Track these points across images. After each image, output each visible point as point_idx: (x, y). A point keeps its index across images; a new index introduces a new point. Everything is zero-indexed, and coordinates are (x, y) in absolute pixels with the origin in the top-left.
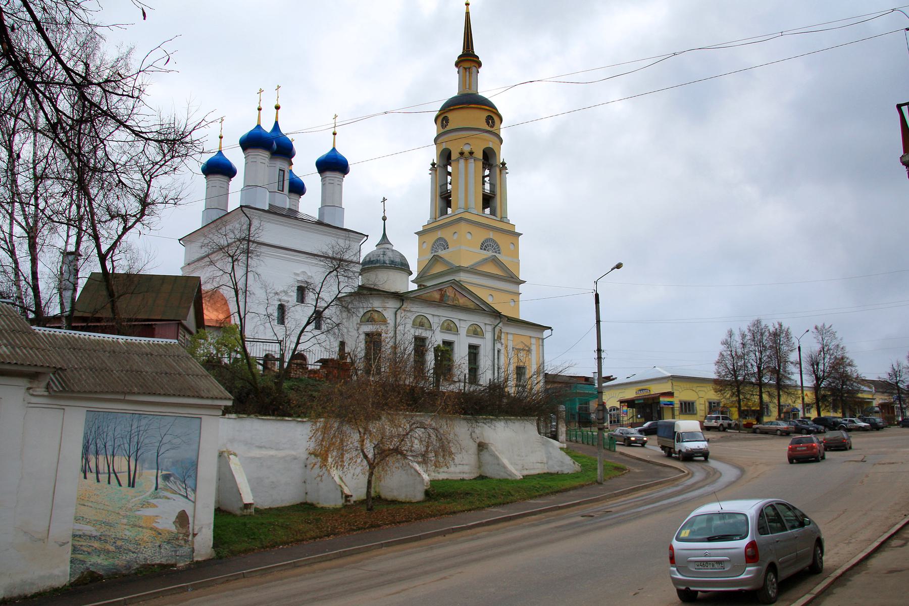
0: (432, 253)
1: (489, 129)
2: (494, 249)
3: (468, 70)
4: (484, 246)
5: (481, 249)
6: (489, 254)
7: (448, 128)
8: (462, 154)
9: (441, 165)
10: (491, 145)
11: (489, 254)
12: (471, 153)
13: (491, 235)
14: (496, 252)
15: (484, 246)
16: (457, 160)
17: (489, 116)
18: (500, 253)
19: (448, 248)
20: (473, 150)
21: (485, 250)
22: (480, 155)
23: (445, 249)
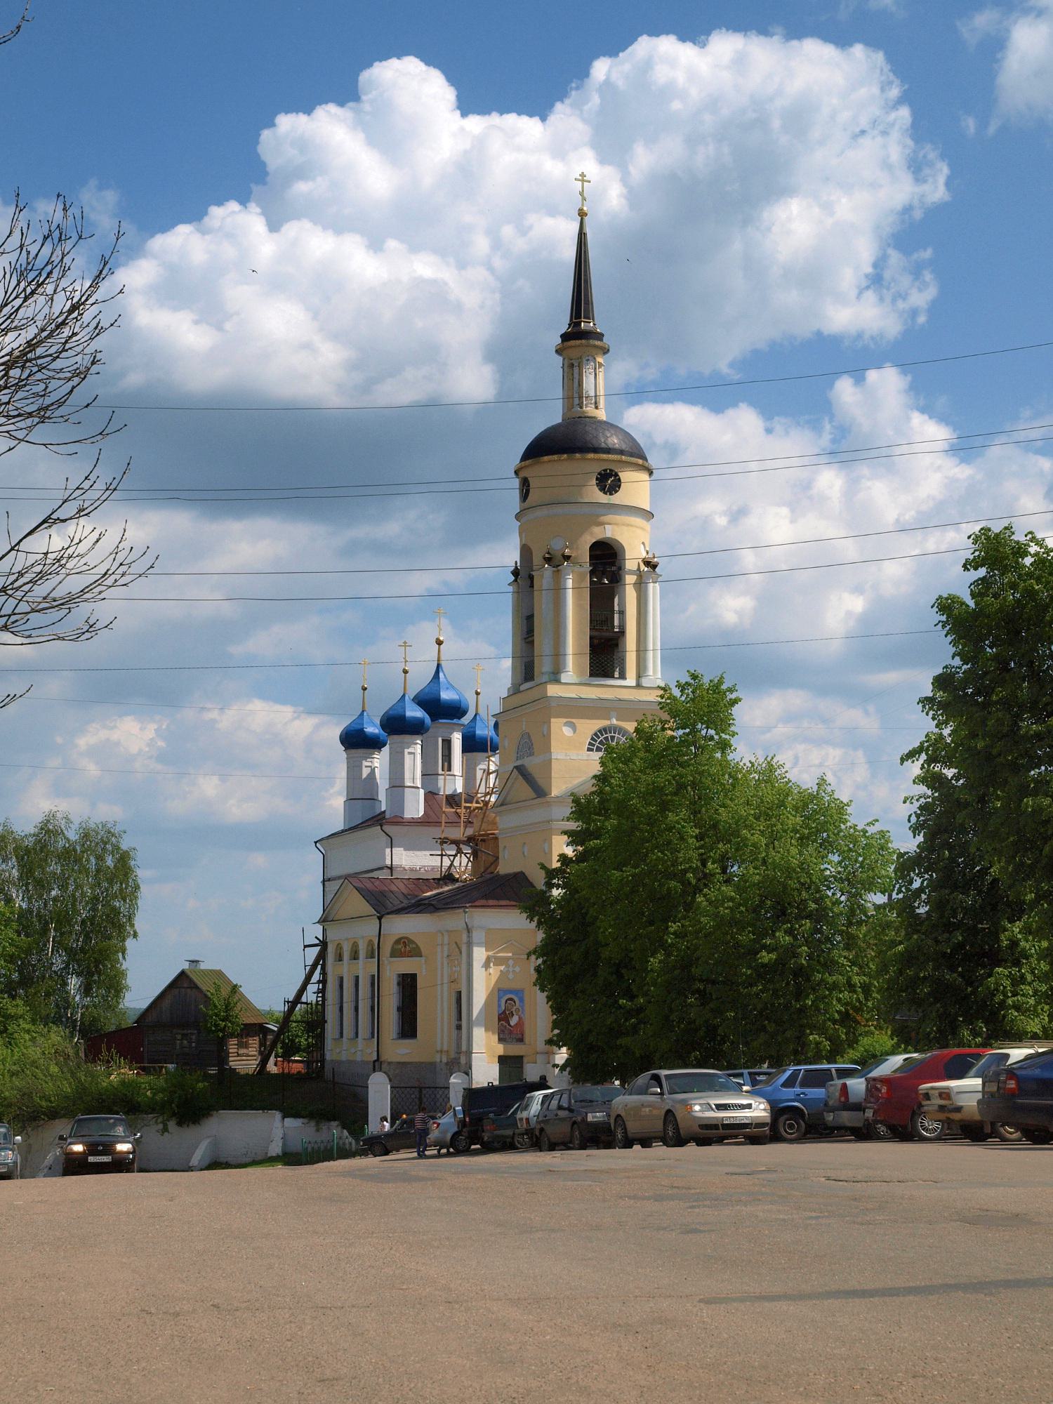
5: (589, 750)
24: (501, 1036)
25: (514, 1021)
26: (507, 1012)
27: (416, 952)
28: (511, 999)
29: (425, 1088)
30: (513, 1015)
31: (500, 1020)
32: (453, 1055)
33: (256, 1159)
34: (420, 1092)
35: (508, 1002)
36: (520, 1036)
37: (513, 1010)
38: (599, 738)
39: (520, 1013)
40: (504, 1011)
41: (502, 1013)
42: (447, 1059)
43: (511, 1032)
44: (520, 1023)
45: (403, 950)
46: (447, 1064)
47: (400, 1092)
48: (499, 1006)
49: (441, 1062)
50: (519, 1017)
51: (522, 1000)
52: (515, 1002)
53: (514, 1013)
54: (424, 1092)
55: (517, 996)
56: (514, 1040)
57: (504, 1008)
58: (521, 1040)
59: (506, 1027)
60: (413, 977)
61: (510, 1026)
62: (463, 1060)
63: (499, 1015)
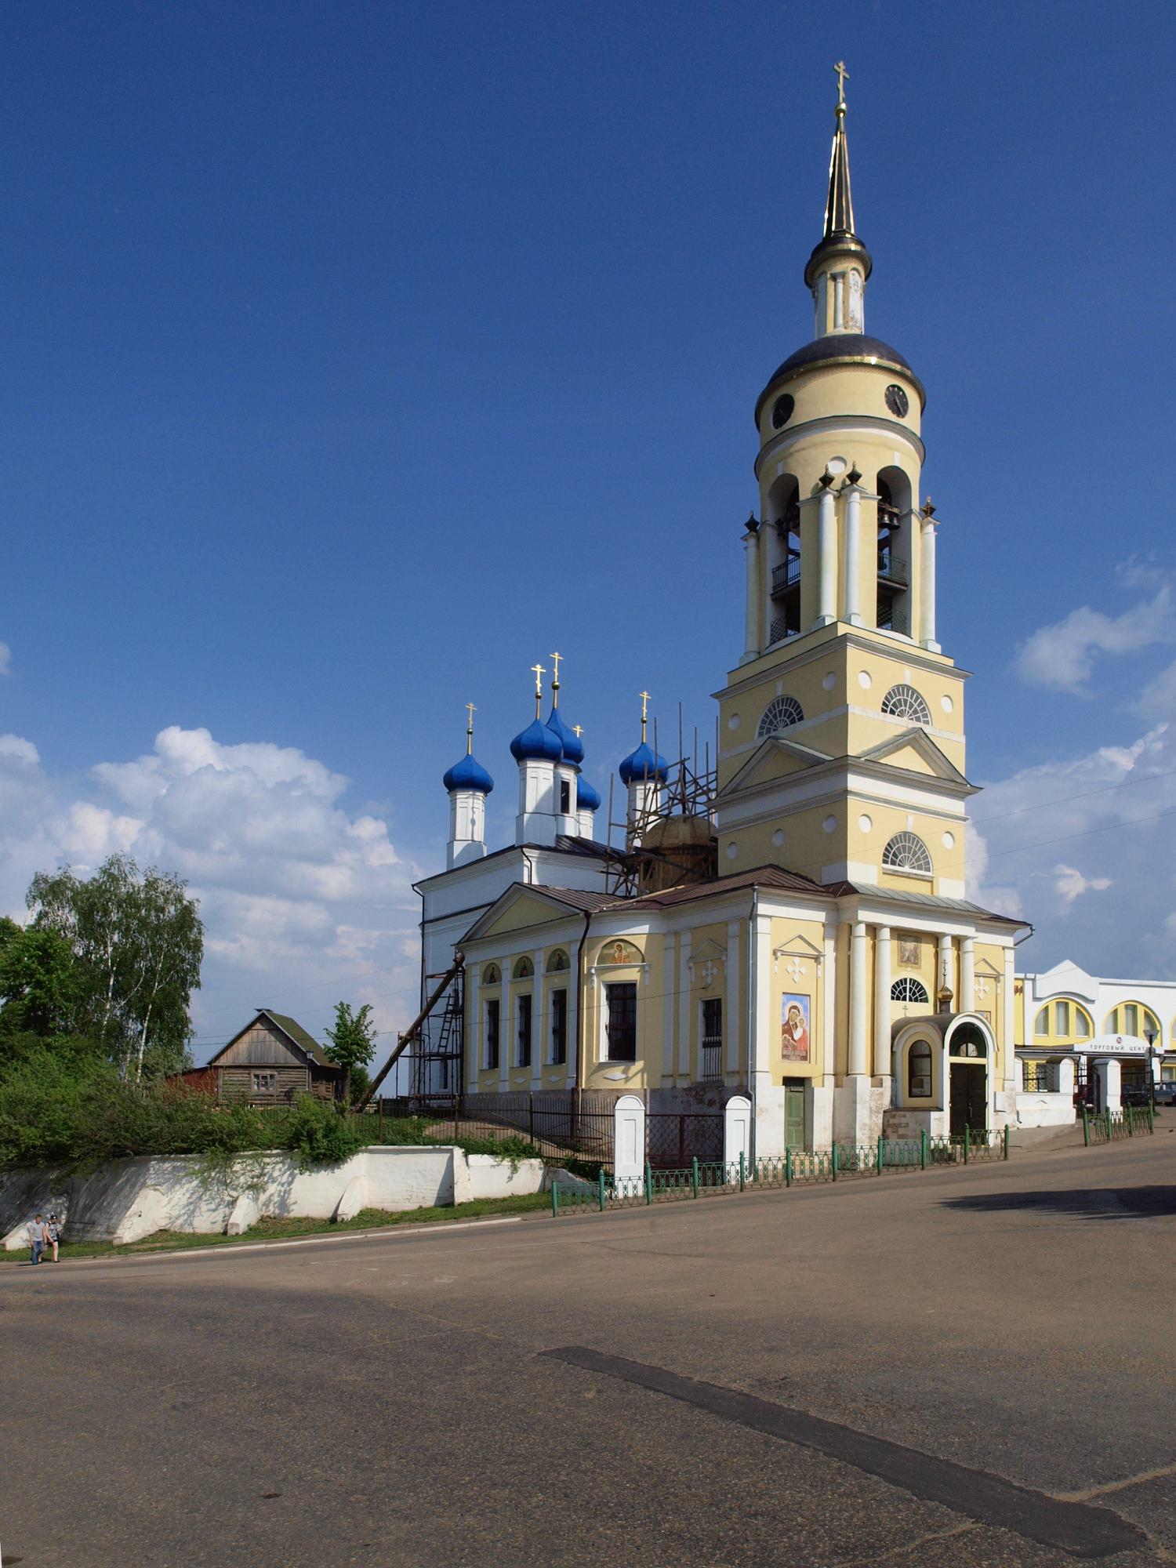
1: (893, 418)
4: (890, 706)
5: (884, 711)
6: (900, 725)
10: (897, 461)
11: (900, 725)
13: (909, 675)
14: (918, 719)
15: (890, 706)
17: (893, 386)
18: (927, 722)
19: (801, 719)
20: (859, 470)
21: (892, 712)
22: (869, 483)
23: (793, 722)
24: (785, 1053)
25: (797, 1034)
26: (791, 1024)
28: (795, 1007)
30: (797, 1027)
31: (784, 1032)
32: (700, 1079)
33: (424, 1206)
35: (792, 1010)
37: (797, 1021)
38: (892, 699)
39: (804, 1025)
40: (787, 1023)
41: (785, 1024)
43: (794, 1048)
44: (803, 1039)
45: (616, 956)
48: (783, 1014)
50: (804, 1031)
52: (799, 1011)
53: (798, 1024)
54: (687, 1121)
58: (804, 1058)
59: (789, 1040)
61: (793, 1039)
62: (730, 1082)
63: (784, 1025)
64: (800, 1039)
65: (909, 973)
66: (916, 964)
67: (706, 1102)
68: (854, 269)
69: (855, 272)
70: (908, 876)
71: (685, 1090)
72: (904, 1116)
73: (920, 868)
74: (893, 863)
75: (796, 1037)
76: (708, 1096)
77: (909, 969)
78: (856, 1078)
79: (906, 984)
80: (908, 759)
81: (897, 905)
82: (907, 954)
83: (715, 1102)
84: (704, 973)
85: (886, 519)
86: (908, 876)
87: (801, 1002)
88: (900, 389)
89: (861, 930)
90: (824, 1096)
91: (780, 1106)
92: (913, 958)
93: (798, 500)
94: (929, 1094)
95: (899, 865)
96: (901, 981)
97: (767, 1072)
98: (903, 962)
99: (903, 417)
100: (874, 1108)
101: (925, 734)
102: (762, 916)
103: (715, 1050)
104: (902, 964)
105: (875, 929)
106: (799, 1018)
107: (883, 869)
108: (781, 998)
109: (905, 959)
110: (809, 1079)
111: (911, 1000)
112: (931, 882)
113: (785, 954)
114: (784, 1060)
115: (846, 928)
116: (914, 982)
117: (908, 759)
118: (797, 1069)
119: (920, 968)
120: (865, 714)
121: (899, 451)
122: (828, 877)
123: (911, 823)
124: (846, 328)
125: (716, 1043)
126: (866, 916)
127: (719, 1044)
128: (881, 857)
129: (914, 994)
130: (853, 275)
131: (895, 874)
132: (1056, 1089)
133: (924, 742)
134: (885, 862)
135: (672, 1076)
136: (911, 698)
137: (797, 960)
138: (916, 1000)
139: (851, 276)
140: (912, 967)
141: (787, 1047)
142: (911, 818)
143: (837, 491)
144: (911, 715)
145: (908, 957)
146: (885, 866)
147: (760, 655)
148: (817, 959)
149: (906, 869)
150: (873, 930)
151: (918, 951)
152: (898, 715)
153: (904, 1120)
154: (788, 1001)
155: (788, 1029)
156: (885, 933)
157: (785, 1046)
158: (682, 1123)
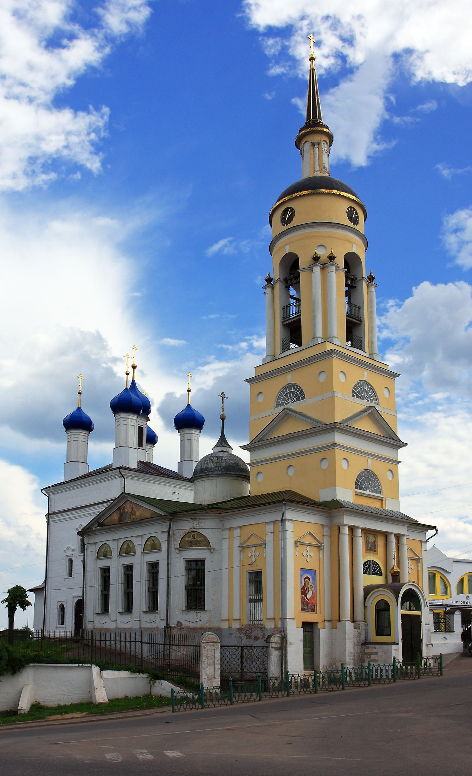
0: (277, 406)
1: (351, 225)
2: (368, 399)
3: (316, 145)
4: (357, 393)
5: (353, 396)
6: (361, 404)
7: (292, 224)
8: (316, 259)
9: (282, 280)
12: (332, 258)
15: (357, 393)
16: (310, 269)
17: (351, 207)
19: (304, 398)
22: (340, 261)
23: (298, 399)
25: (309, 595)
26: (306, 588)
27: (205, 544)
28: (307, 578)
29: (247, 647)
34: (242, 650)
35: (306, 579)
36: (313, 607)
37: (309, 586)
39: (313, 589)
40: (304, 587)
42: (240, 625)
43: (308, 604)
44: (314, 597)
46: (240, 629)
47: (230, 650)
49: (230, 628)
51: (314, 579)
55: (311, 576)
56: (310, 610)
57: (303, 585)
58: (314, 610)
60: (203, 562)
61: (307, 598)
63: (301, 589)
64: (311, 598)
65: (371, 557)
66: (375, 551)
67: (253, 637)
68: (324, 141)
69: (325, 143)
70: (369, 497)
71: (238, 629)
72: (375, 648)
73: (375, 492)
74: (361, 489)
75: (309, 597)
76: (253, 635)
77: (371, 554)
78: (345, 623)
79: (370, 564)
80: (366, 425)
81: (365, 514)
82: (370, 545)
83: (259, 637)
84: (250, 555)
85: (349, 282)
86: (369, 497)
87: (311, 574)
88: (354, 209)
89: (346, 530)
90: (323, 633)
91: (301, 641)
92: (373, 547)
93: (299, 269)
94: (389, 634)
95: (364, 490)
96: (367, 561)
97: (293, 619)
98: (368, 550)
99: (356, 225)
100: (356, 643)
101: (377, 410)
102: (289, 520)
103: (257, 604)
104: (368, 551)
105: (352, 529)
106: (310, 585)
107: (355, 492)
108: (299, 572)
109: (369, 548)
110: (317, 623)
111: (373, 574)
112: (382, 500)
113: (302, 544)
114: (302, 612)
115: (337, 528)
116: (374, 562)
117: (366, 425)
118: (310, 617)
119: (377, 554)
120: (343, 398)
121: (355, 244)
122: (324, 496)
123: (372, 464)
124: (321, 172)
125: (260, 599)
126: (349, 520)
127: (260, 600)
128: (354, 485)
129: (374, 570)
130: (324, 144)
131: (361, 495)
132: (451, 629)
133: (377, 415)
134: (356, 488)
135: (222, 620)
136: (368, 389)
137: (308, 548)
138: (376, 574)
139: (323, 144)
140: (373, 554)
141: (303, 603)
142: (370, 461)
143: (322, 264)
144: (368, 399)
145: (371, 547)
146: (357, 490)
147: (274, 359)
148: (319, 547)
149: (368, 492)
150: (352, 529)
151: (376, 543)
152: (361, 398)
153: (374, 650)
154: (303, 575)
155: (304, 591)
156: (359, 532)
157: (302, 603)
158: (242, 650)
